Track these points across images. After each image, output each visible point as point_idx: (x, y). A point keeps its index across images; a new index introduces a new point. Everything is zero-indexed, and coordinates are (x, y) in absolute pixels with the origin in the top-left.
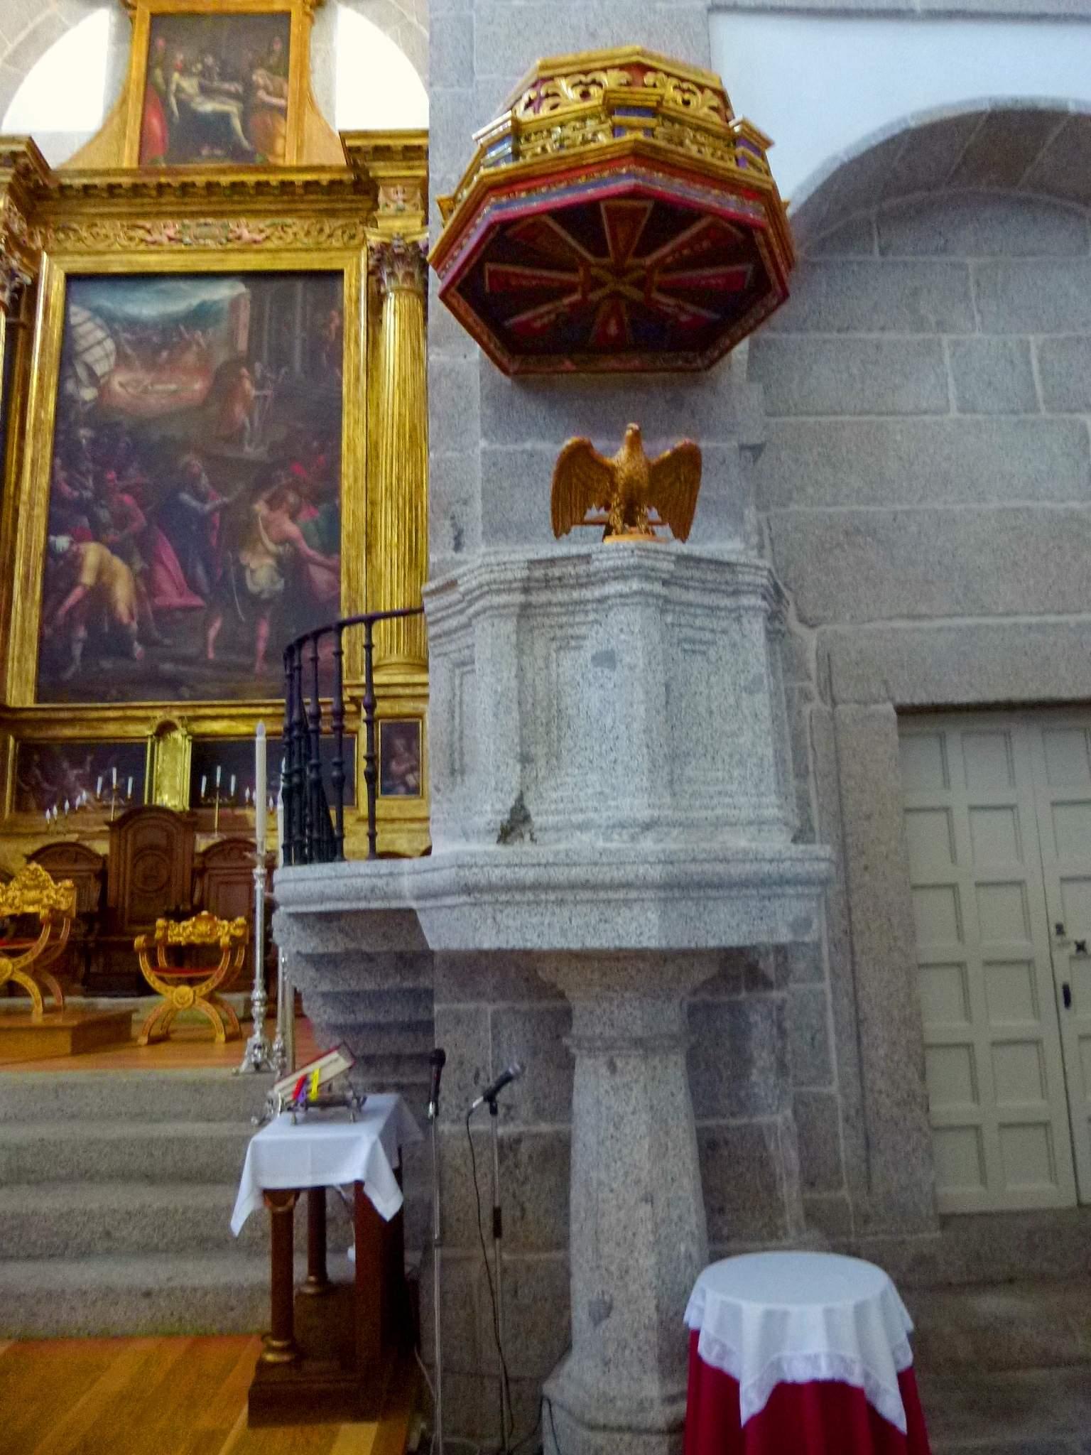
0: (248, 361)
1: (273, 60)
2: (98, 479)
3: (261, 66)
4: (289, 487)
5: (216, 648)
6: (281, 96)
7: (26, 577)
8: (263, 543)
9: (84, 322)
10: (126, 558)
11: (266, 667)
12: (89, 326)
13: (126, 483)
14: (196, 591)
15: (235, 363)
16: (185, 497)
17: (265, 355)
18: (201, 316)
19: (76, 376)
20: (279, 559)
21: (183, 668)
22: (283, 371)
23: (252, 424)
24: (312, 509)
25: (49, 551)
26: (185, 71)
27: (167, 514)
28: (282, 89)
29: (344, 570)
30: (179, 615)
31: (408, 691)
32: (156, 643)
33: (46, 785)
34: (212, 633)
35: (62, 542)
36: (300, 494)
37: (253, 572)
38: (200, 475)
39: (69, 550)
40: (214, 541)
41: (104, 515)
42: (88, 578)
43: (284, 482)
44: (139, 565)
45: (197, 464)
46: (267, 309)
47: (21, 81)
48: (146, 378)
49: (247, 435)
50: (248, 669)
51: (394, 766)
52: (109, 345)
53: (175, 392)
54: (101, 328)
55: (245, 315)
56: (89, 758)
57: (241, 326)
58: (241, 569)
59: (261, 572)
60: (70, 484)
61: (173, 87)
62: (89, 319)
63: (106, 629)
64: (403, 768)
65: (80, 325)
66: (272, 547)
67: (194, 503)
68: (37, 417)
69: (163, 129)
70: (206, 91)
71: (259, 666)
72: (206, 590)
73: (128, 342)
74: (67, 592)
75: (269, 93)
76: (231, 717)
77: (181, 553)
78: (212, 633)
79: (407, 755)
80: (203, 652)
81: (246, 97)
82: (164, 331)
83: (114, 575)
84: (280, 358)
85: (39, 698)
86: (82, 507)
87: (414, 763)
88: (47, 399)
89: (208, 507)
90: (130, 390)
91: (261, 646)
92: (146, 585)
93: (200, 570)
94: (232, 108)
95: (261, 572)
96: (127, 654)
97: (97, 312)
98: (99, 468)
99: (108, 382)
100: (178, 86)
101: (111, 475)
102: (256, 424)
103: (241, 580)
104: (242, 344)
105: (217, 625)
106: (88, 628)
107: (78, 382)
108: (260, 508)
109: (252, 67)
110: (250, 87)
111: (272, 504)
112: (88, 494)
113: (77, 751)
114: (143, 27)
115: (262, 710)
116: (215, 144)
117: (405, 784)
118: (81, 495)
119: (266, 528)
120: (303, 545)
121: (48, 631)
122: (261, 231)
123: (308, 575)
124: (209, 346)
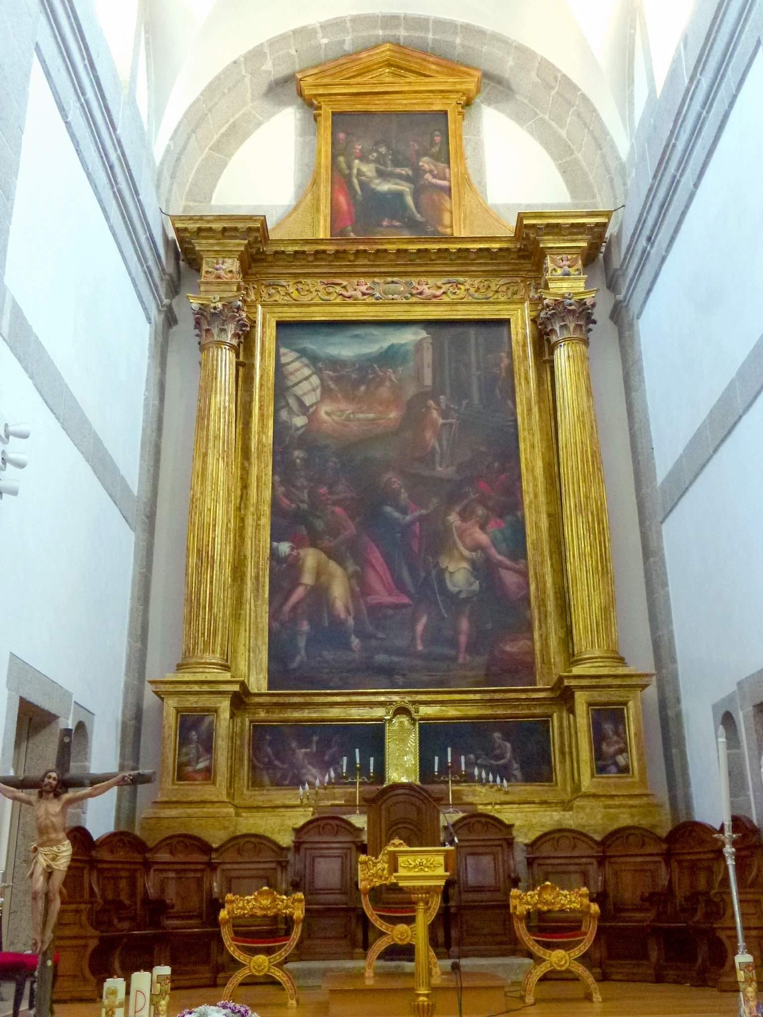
0: (434, 393)
1: (435, 149)
3: (426, 154)
6: (444, 179)
7: (257, 577)
8: (458, 549)
9: (292, 362)
10: (341, 563)
11: (468, 658)
12: (297, 364)
13: (335, 497)
15: (422, 396)
16: (388, 509)
17: (448, 390)
18: (389, 357)
19: (288, 404)
20: (473, 563)
21: (395, 659)
22: (464, 402)
23: (441, 446)
24: (498, 520)
25: (274, 555)
26: (363, 158)
28: (444, 174)
29: (531, 573)
30: (390, 612)
31: (618, 682)
32: (371, 636)
33: (277, 763)
34: (420, 628)
35: (284, 548)
37: (451, 573)
39: (290, 555)
40: (416, 548)
41: (320, 525)
42: (308, 579)
44: (352, 567)
46: (447, 351)
47: (226, 164)
48: (348, 408)
49: (437, 457)
50: (454, 659)
51: (604, 747)
52: (315, 380)
53: (373, 420)
54: (306, 365)
55: (428, 357)
56: (315, 738)
57: (425, 365)
58: (441, 572)
59: (458, 574)
60: (286, 496)
61: (355, 171)
62: (297, 359)
63: (327, 624)
64: (612, 749)
65: (288, 364)
66: (466, 553)
67: (397, 515)
68: (260, 441)
69: (348, 205)
70: (382, 175)
71: (463, 658)
73: (331, 378)
75: (434, 177)
76: (442, 703)
78: (420, 628)
79: (615, 738)
81: (415, 178)
82: (360, 369)
83: (331, 576)
84: (461, 392)
85: (272, 683)
86: (299, 518)
87: (622, 745)
88: (267, 427)
89: (408, 518)
90: (335, 418)
91: (463, 639)
93: (406, 575)
94: (405, 188)
95: (458, 574)
96: (347, 646)
97: (303, 353)
99: (315, 412)
100: (359, 170)
101: (324, 490)
103: (441, 581)
104: (428, 381)
105: (424, 620)
106: (311, 622)
107: (291, 412)
108: (454, 518)
109: (419, 155)
110: (418, 172)
111: (464, 515)
112: (304, 506)
113: (304, 732)
114: (326, 123)
115: (471, 697)
116: (393, 217)
117: (616, 764)
119: (461, 537)
120: (493, 551)
121: (276, 625)
122: (440, 288)
123: (500, 579)
124: (400, 380)
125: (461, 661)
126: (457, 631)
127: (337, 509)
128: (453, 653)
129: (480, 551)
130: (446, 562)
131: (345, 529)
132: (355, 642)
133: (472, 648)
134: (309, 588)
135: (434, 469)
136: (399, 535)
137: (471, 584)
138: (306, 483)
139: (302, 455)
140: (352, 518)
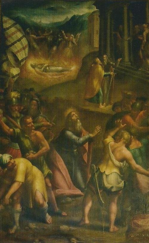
2: (23, 122)
4: (123, 128)
5: (90, 218)
8: (112, 160)
10: (40, 168)
11: (116, 229)
13: (36, 125)
14: (78, 186)
16: (69, 133)
20: (120, 169)
21: (72, 228)
24: (137, 142)
27: (62, 143)
30: (69, 199)
36: (131, 134)
37: (107, 176)
38: (76, 122)
39: (9, 162)
41: (27, 143)
42: (20, 178)
43: (122, 126)
44: (47, 171)
45: (75, 116)
49: (101, 98)
50: (107, 229)
59: (111, 176)
60: (7, 124)
66: (117, 163)
67: (74, 137)
71: (113, 228)
72: (83, 186)
74: (9, 186)
77: (68, 164)
78: (87, 209)
80: (83, 220)
83: (34, 177)
89: (82, 139)
92: (52, 183)
95: (111, 176)
98: (22, 115)
101: (29, 120)
102: (106, 92)
105: (90, 205)
108: (109, 140)
111: (116, 138)
112: (18, 130)
118: (14, 130)
119: (113, 152)
120: (133, 162)
125: (111, 230)
126: (109, 211)
127: (39, 134)
128: (107, 225)
129: (125, 162)
130: (103, 168)
131: (43, 146)
132: (49, 218)
133: (118, 222)
134: (21, 184)
135: (99, 107)
136: (76, 150)
137: (119, 183)
138: (19, 115)
139: (16, 96)
140: (47, 138)
